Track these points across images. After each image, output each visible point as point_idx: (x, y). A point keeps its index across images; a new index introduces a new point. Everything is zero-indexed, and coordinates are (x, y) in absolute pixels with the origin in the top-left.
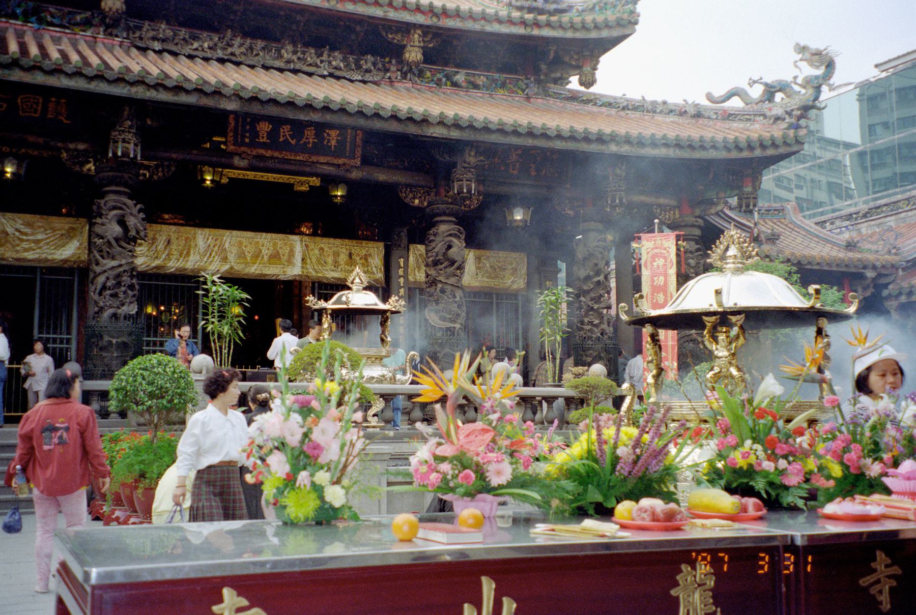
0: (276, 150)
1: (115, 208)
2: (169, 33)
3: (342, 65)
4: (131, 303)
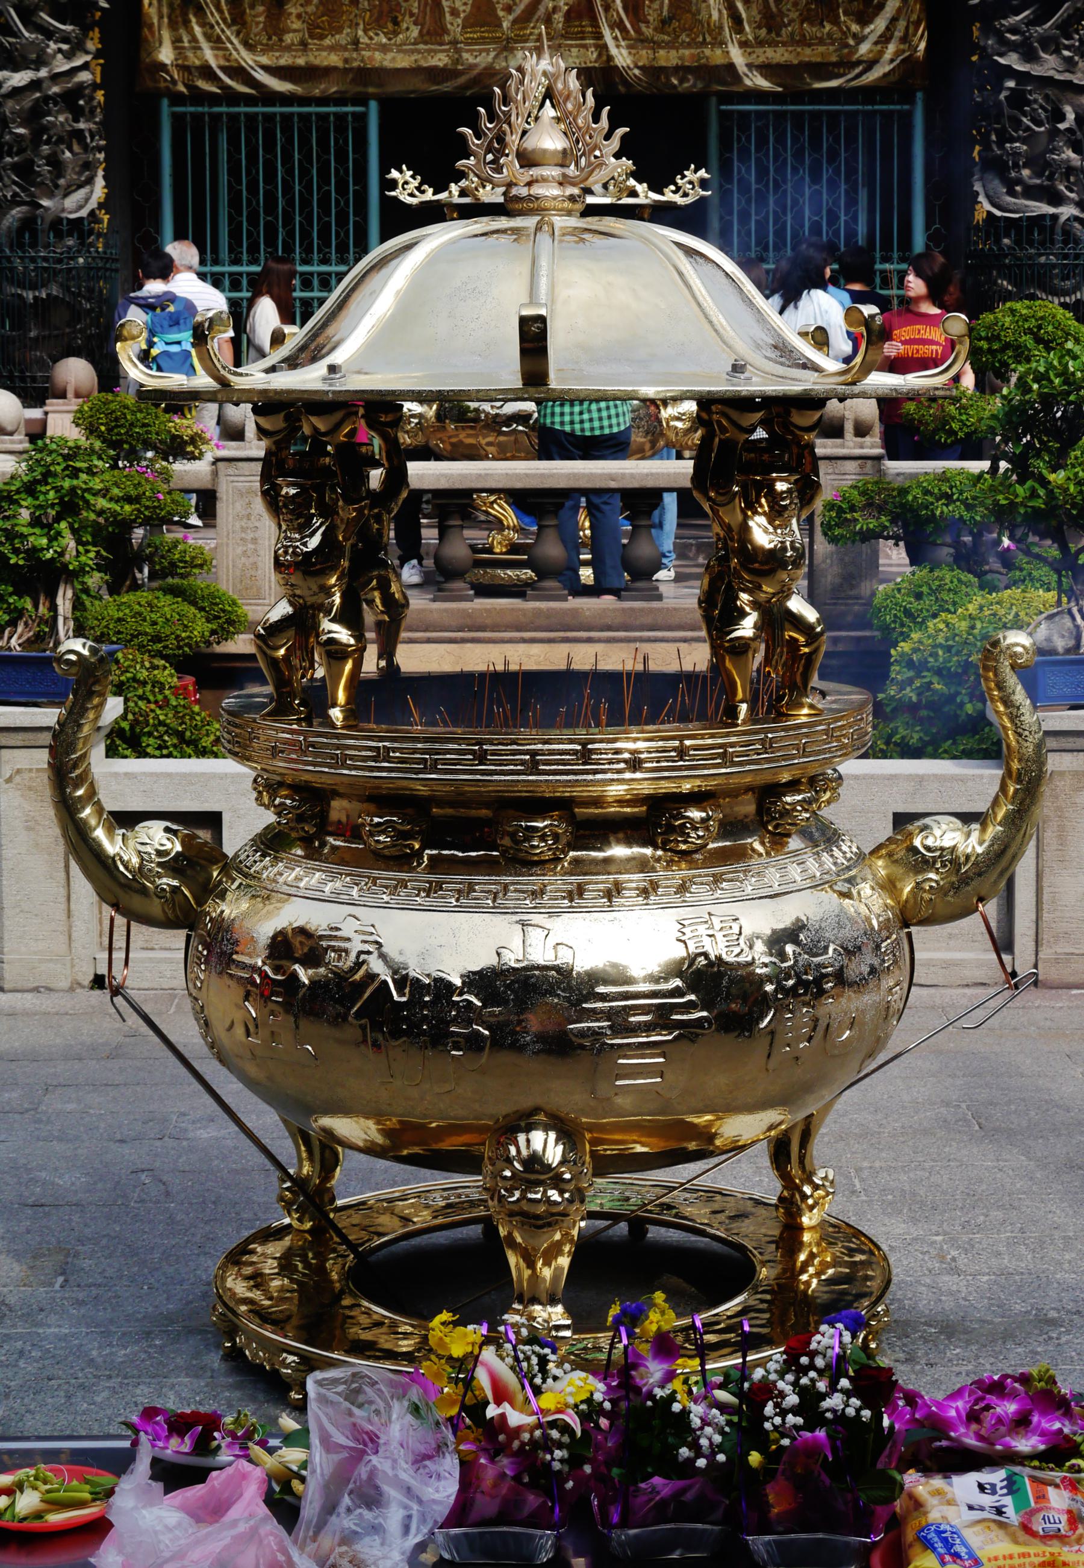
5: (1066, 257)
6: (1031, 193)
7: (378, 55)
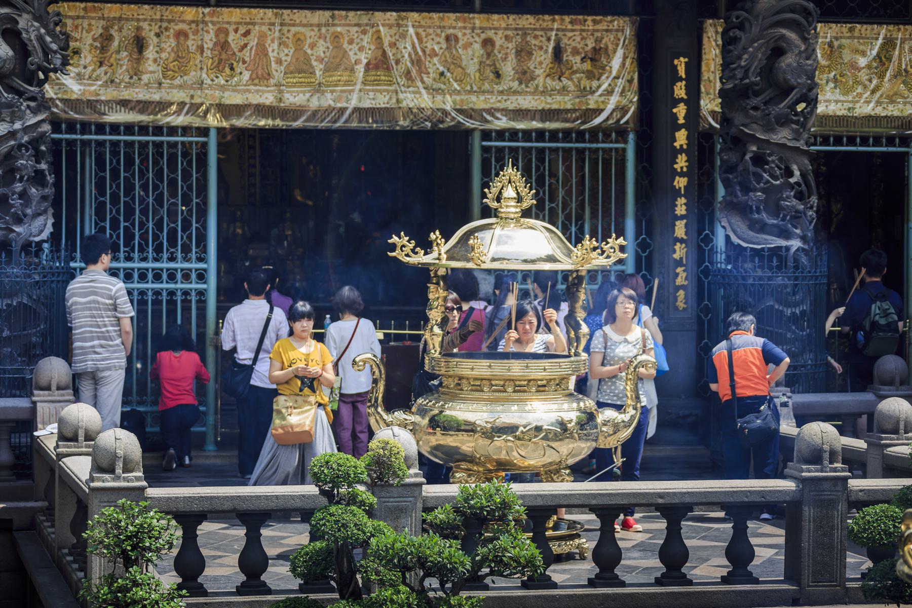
4: (37, 215)
5: (796, 278)
6: (762, 228)
7: (217, 93)
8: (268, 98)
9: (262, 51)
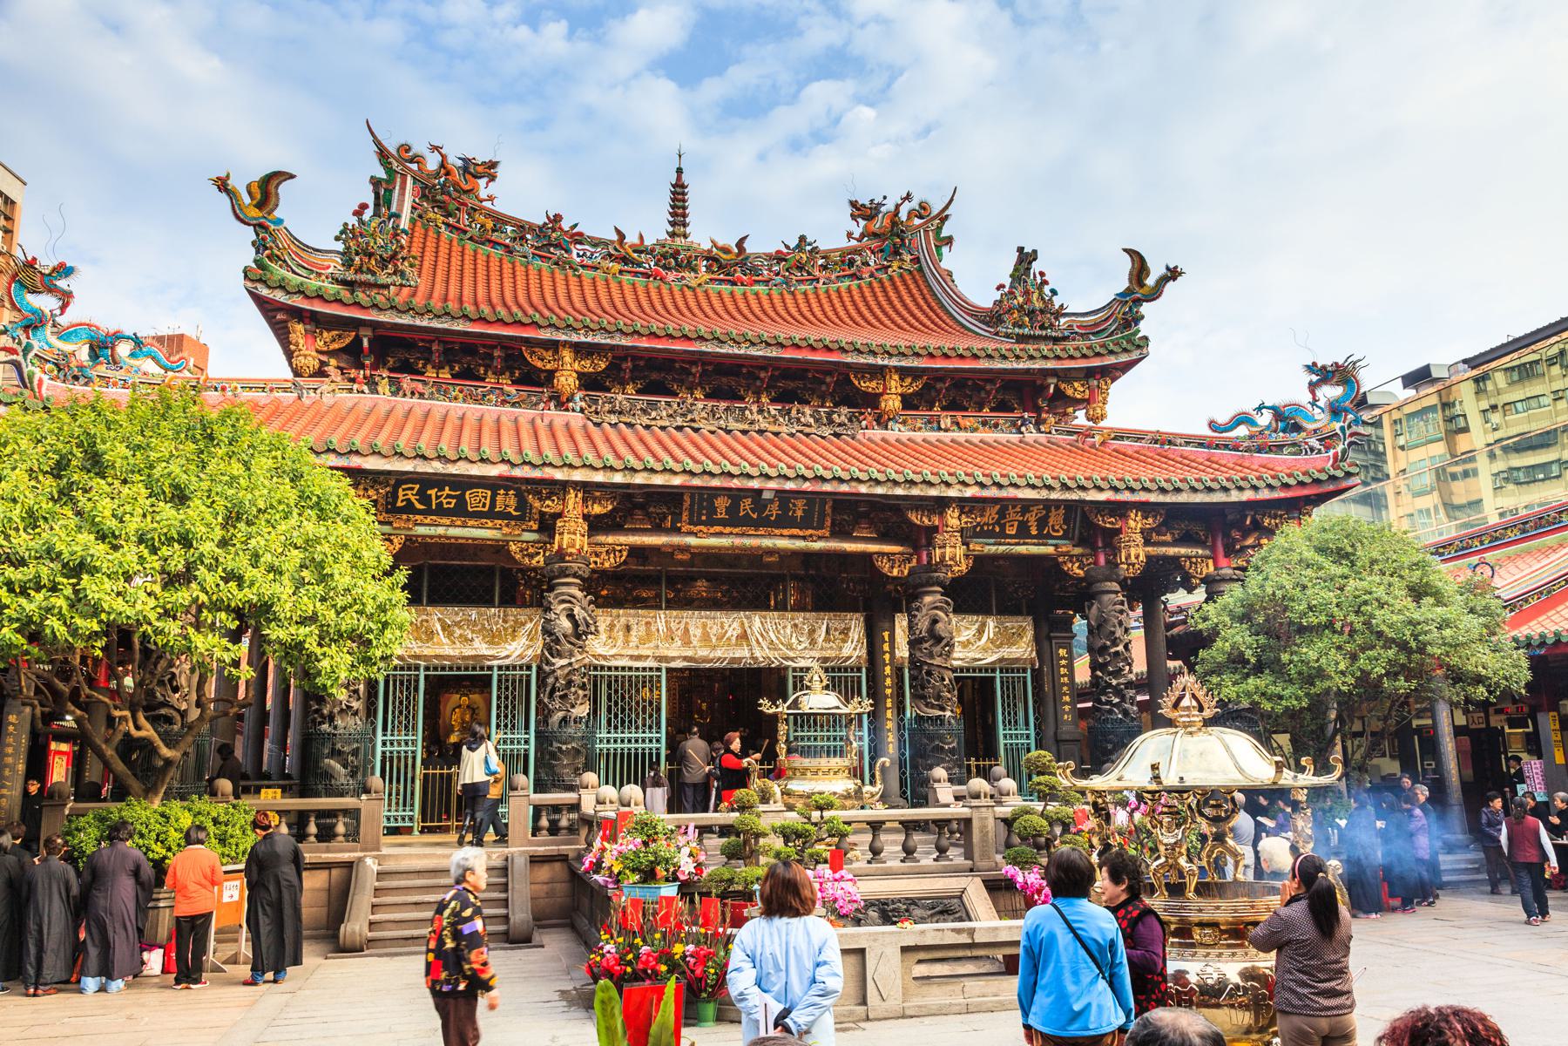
0: (735, 526)
1: (563, 601)
2: (627, 405)
3: (812, 420)
6: (933, 707)
8: (690, 653)
9: (686, 630)
